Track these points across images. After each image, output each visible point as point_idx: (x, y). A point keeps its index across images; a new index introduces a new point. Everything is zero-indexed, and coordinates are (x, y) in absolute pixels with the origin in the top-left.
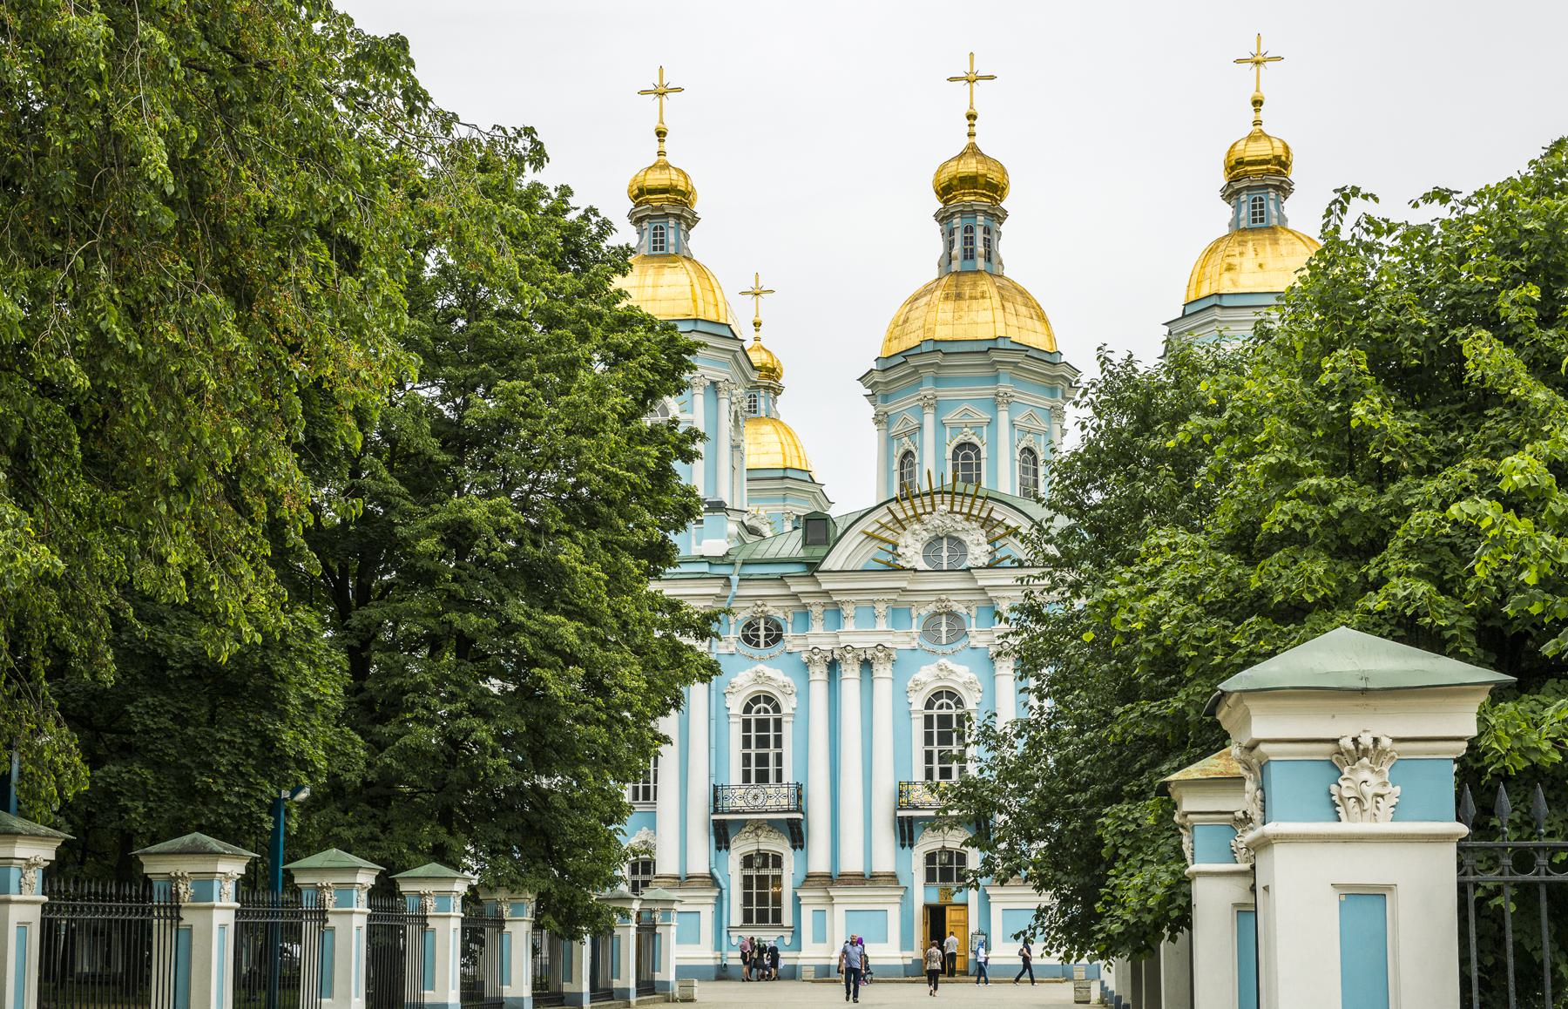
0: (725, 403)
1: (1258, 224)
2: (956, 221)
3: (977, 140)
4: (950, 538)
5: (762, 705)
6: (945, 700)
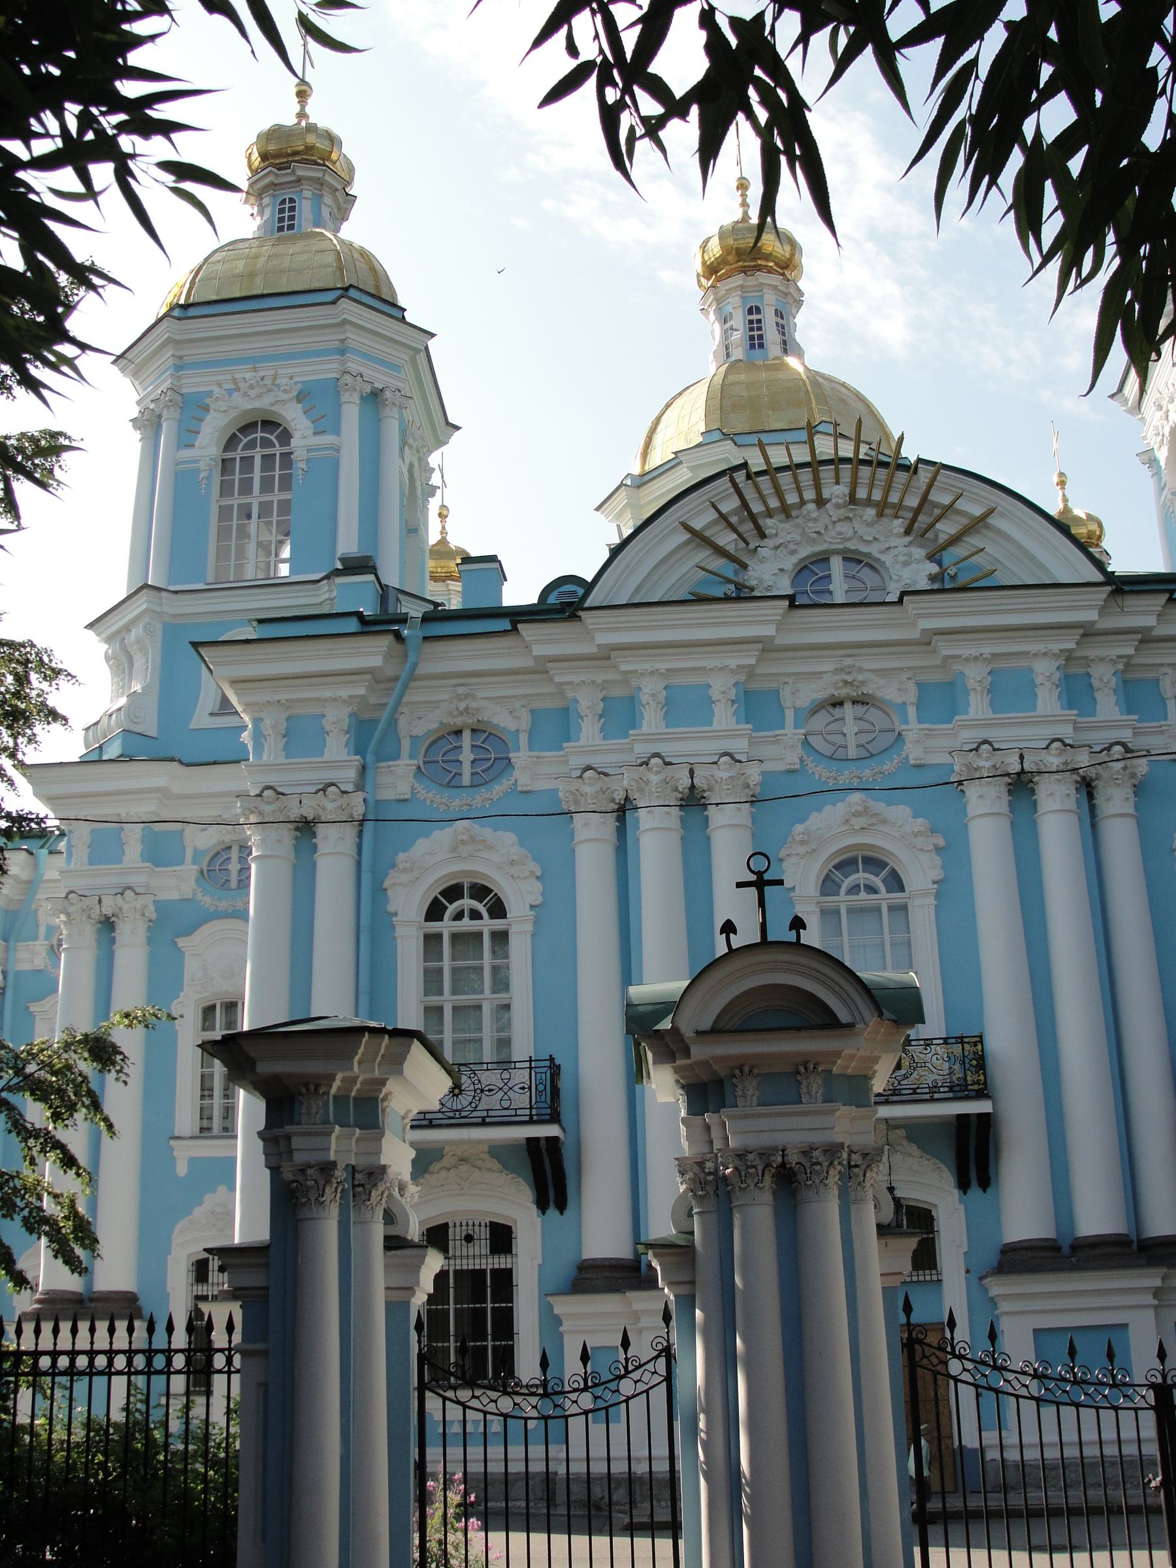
4: (852, 558)
5: (467, 903)
6: (861, 876)
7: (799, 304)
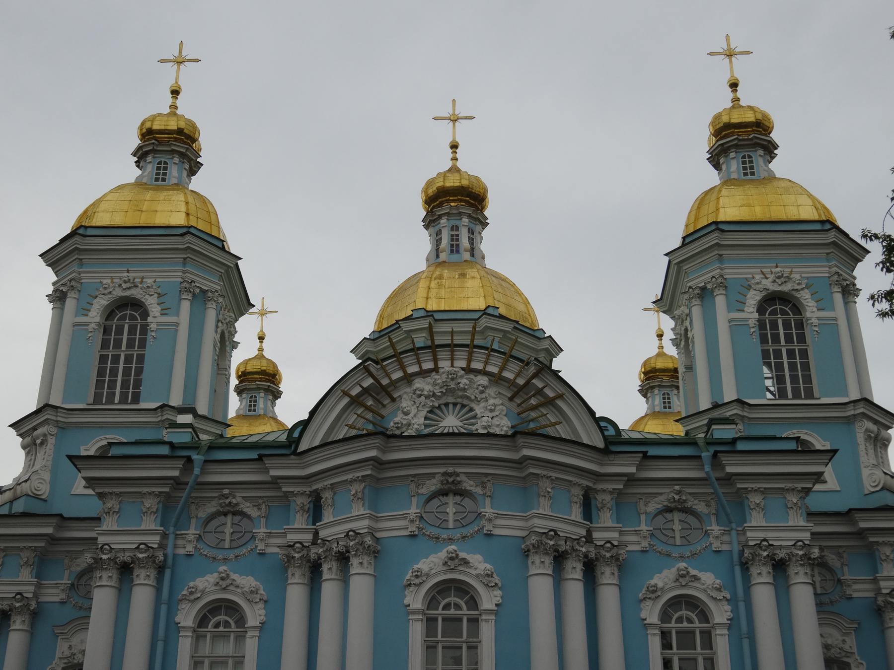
0: (211, 315)
1: (749, 177)
2: (443, 221)
3: (459, 164)
5: (222, 617)
7: (485, 225)
